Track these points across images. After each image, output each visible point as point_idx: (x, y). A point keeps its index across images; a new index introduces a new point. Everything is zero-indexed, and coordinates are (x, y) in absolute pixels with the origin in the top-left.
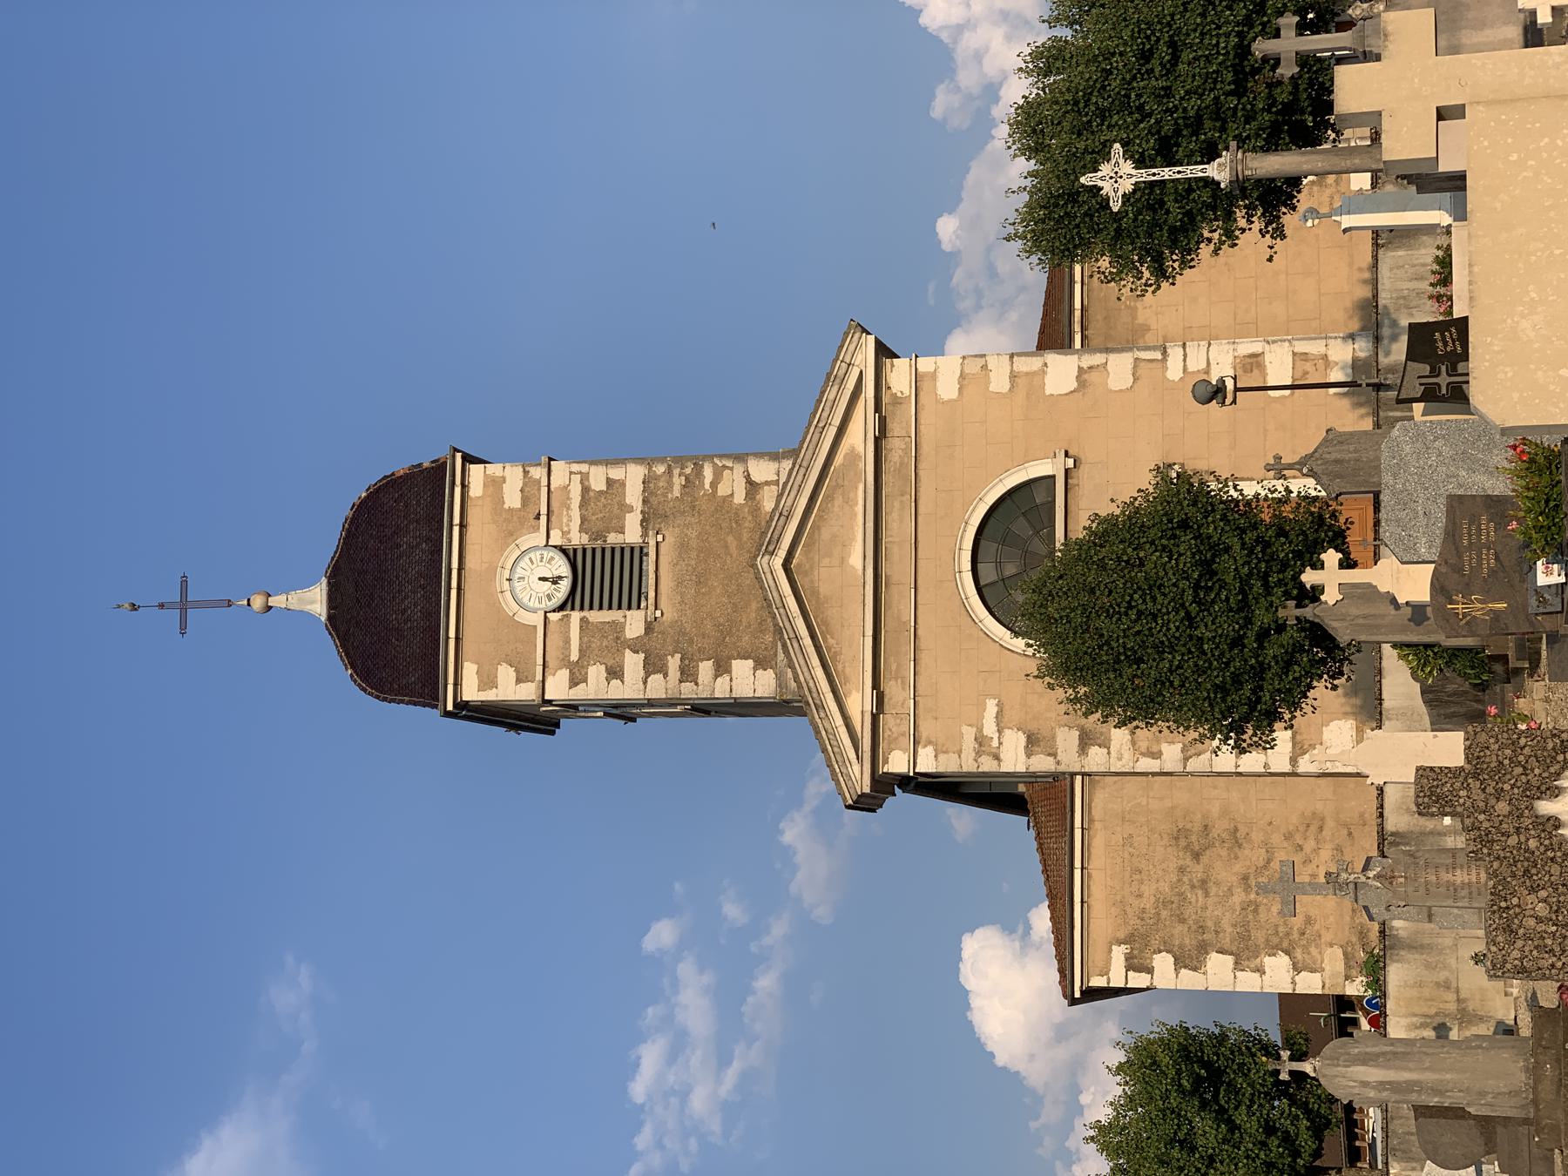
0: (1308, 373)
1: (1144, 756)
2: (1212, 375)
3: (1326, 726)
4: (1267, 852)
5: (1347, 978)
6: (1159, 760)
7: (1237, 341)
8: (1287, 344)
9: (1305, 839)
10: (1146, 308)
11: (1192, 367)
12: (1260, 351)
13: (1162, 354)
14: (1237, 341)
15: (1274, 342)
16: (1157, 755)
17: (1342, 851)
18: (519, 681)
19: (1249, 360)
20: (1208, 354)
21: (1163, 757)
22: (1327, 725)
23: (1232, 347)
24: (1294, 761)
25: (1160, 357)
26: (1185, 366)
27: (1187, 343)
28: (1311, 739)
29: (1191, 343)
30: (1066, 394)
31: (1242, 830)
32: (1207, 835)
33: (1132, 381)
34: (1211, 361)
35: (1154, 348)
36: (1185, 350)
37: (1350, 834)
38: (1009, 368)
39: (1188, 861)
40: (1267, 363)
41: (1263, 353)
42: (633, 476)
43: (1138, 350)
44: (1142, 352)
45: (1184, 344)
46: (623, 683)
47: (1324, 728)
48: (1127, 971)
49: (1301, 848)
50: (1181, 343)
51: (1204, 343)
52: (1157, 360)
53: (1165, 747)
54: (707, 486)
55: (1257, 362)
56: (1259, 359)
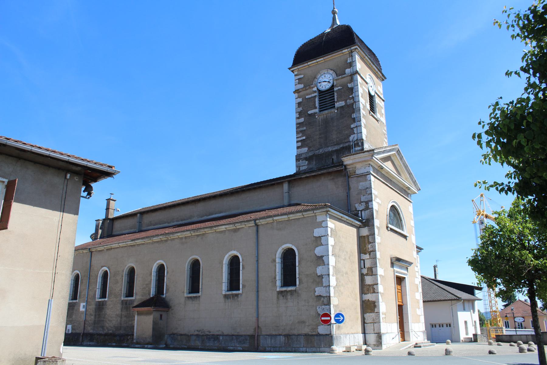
5: (334, 305)
18: (359, 69)
42: (383, 119)
48: (331, 228)
54: (385, 139)
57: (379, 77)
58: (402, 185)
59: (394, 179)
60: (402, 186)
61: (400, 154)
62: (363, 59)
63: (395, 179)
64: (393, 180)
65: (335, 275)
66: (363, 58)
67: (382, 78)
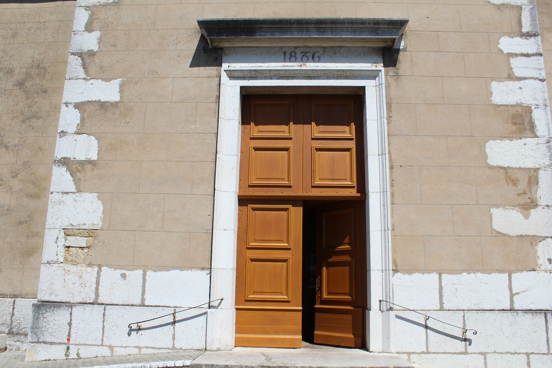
1: (90, 16)
2: (507, 82)
3: (98, 197)
4: (15, 146)
6: (84, 29)
7: (548, 108)
9: (22, 180)
11: (515, 63)
12: (538, 133)
13: (528, 32)
14: (548, 108)
16: (89, 28)
17: (6, 214)
19: (526, 121)
20: (531, 78)
21: (87, 34)
22: (99, 198)
23: (541, 103)
24: (65, 162)
25: (524, 30)
26: (516, 55)
27: (542, 58)
28: (86, 180)
29: (543, 61)
31: (36, 123)
32: (38, 93)
33: (496, 3)
34: (522, 82)
35: (533, 24)
36: (533, 55)
37: (21, 223)
39: (17, 77)
40: (524, 140)
41: (536, 136)
43: (531, 9)
44: (528, 14)
45: (541, 55)
47: (96, 195)
49: (14, 175)
50: (541, 51)
51: (543, 75)
52: (521, 26)
53: (96, 34)
55: (525, 129)
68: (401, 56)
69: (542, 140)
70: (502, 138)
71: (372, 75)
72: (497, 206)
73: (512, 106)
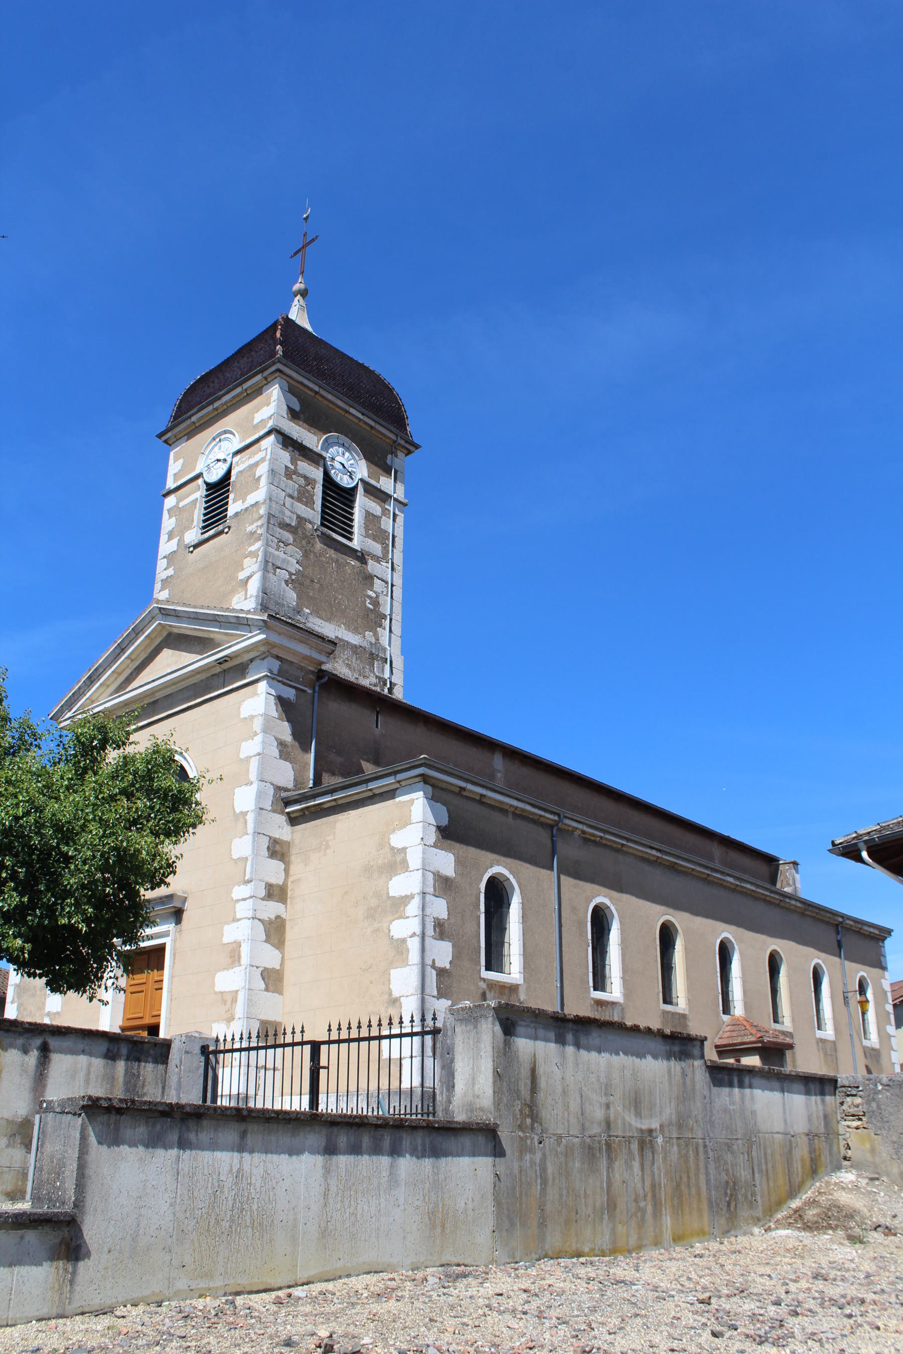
0: (225, 1004)
8: (243, 985)
10: (319, 859)
12: (242, 963)
15: (246, 973)
30: (233, 806)
36: (248, 898)
38: (252, 754)
40: (235, 969)
46: (167, 542)
56: (237, 963)
57: (265, 382)
58: (198, 673)
59: (157, 694)
60: (203, 676)
61: (167, 612)
62: (196, 427)
63: (157, 691)
64: (158, 696)
65: (16, 999)
66: (194, 427)
67: (272, 373)
68: (185, 916)
69: (243, 968)
70: (224, 969)
71: (166, 934)
72: (215, 1021)
73: (232, 943)
